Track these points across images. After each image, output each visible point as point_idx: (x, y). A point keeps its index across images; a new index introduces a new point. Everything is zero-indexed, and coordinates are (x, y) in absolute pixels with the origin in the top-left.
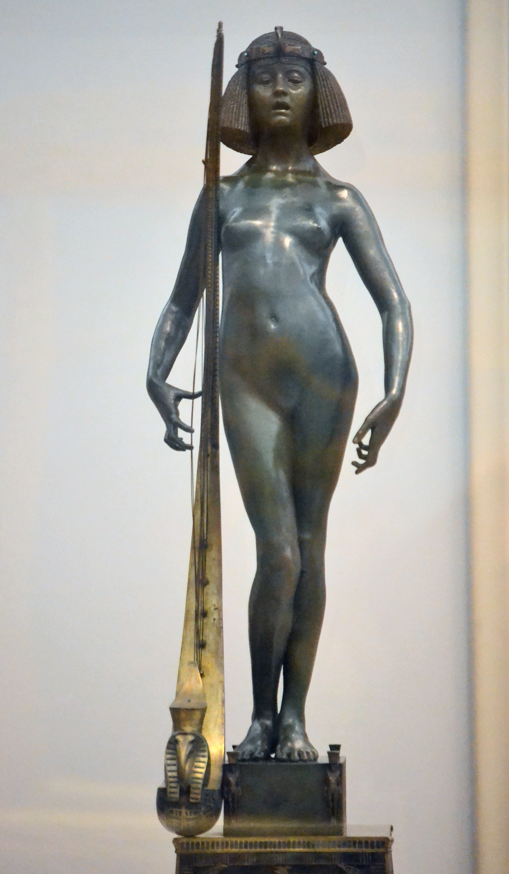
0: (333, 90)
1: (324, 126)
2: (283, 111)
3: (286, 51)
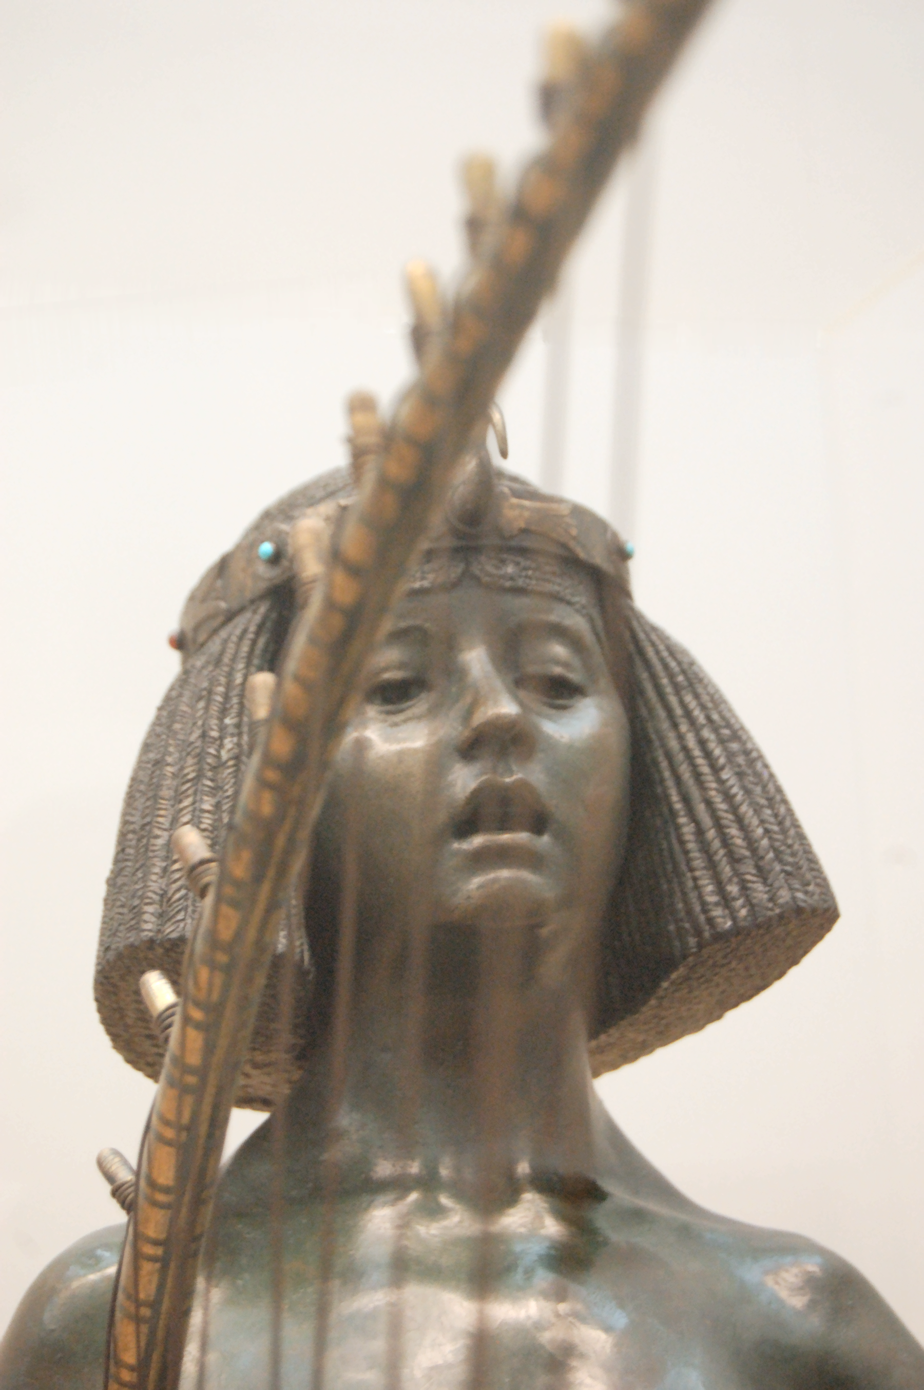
2: (522, 837)
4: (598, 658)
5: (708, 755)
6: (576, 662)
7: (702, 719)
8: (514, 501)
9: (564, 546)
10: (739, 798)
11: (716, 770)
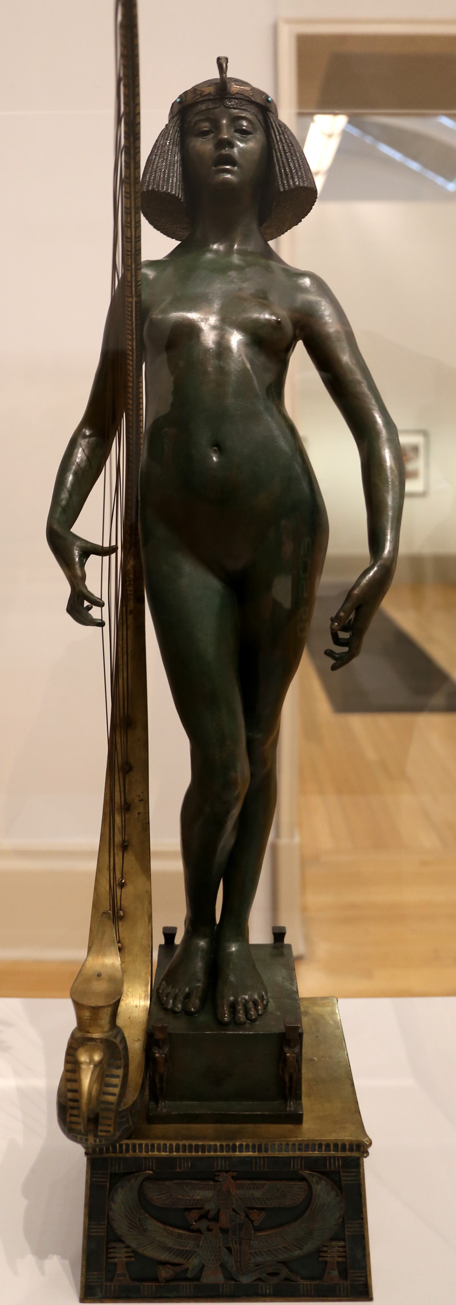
0: (292, 145)
1: (282, 190)
3: (231, 92)
4: (258, 125)
5: (284, 150)
6: (250, 126)
7: (284, 142)
8: (235, 86)
9: (248, 97)
10: (290, 160)
11: (285, 153)
